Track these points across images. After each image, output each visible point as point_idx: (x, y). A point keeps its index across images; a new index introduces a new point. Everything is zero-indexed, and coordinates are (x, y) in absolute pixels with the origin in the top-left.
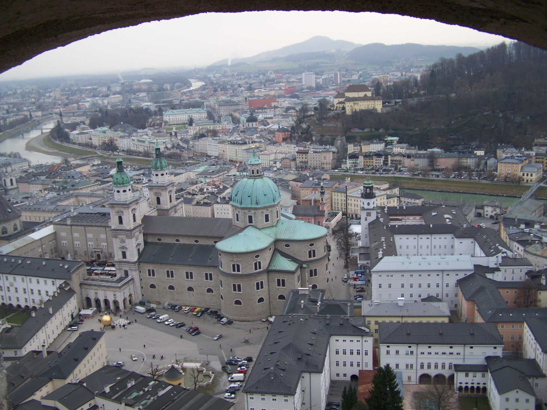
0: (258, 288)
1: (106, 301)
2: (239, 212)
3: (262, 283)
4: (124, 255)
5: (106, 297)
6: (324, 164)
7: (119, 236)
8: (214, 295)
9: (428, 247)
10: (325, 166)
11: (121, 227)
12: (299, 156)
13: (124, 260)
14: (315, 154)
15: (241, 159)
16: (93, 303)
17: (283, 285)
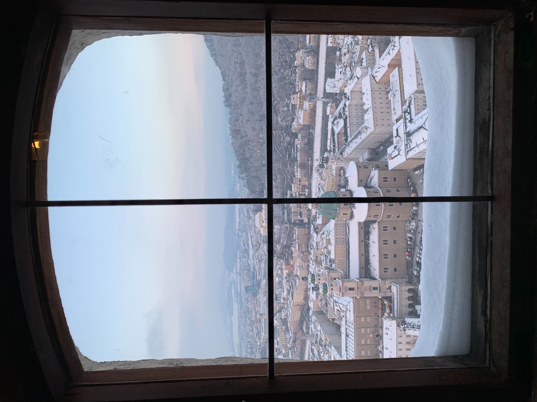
0: (391, 192)
1: (409, 298)
2: (341, 212)
3: (386, 190)
4: (375, 289)
5: (406, 298)
6: (305, 233)
7: (362, 291)
8: (397, 225)
9: (357, 119)
10: (307, 233)
11: (356, 289)
12: (301, 249)
13: (379, 289)
14: (299, 239)
15: (303, 291)
16: (411, 310)
17: (387, 178)
